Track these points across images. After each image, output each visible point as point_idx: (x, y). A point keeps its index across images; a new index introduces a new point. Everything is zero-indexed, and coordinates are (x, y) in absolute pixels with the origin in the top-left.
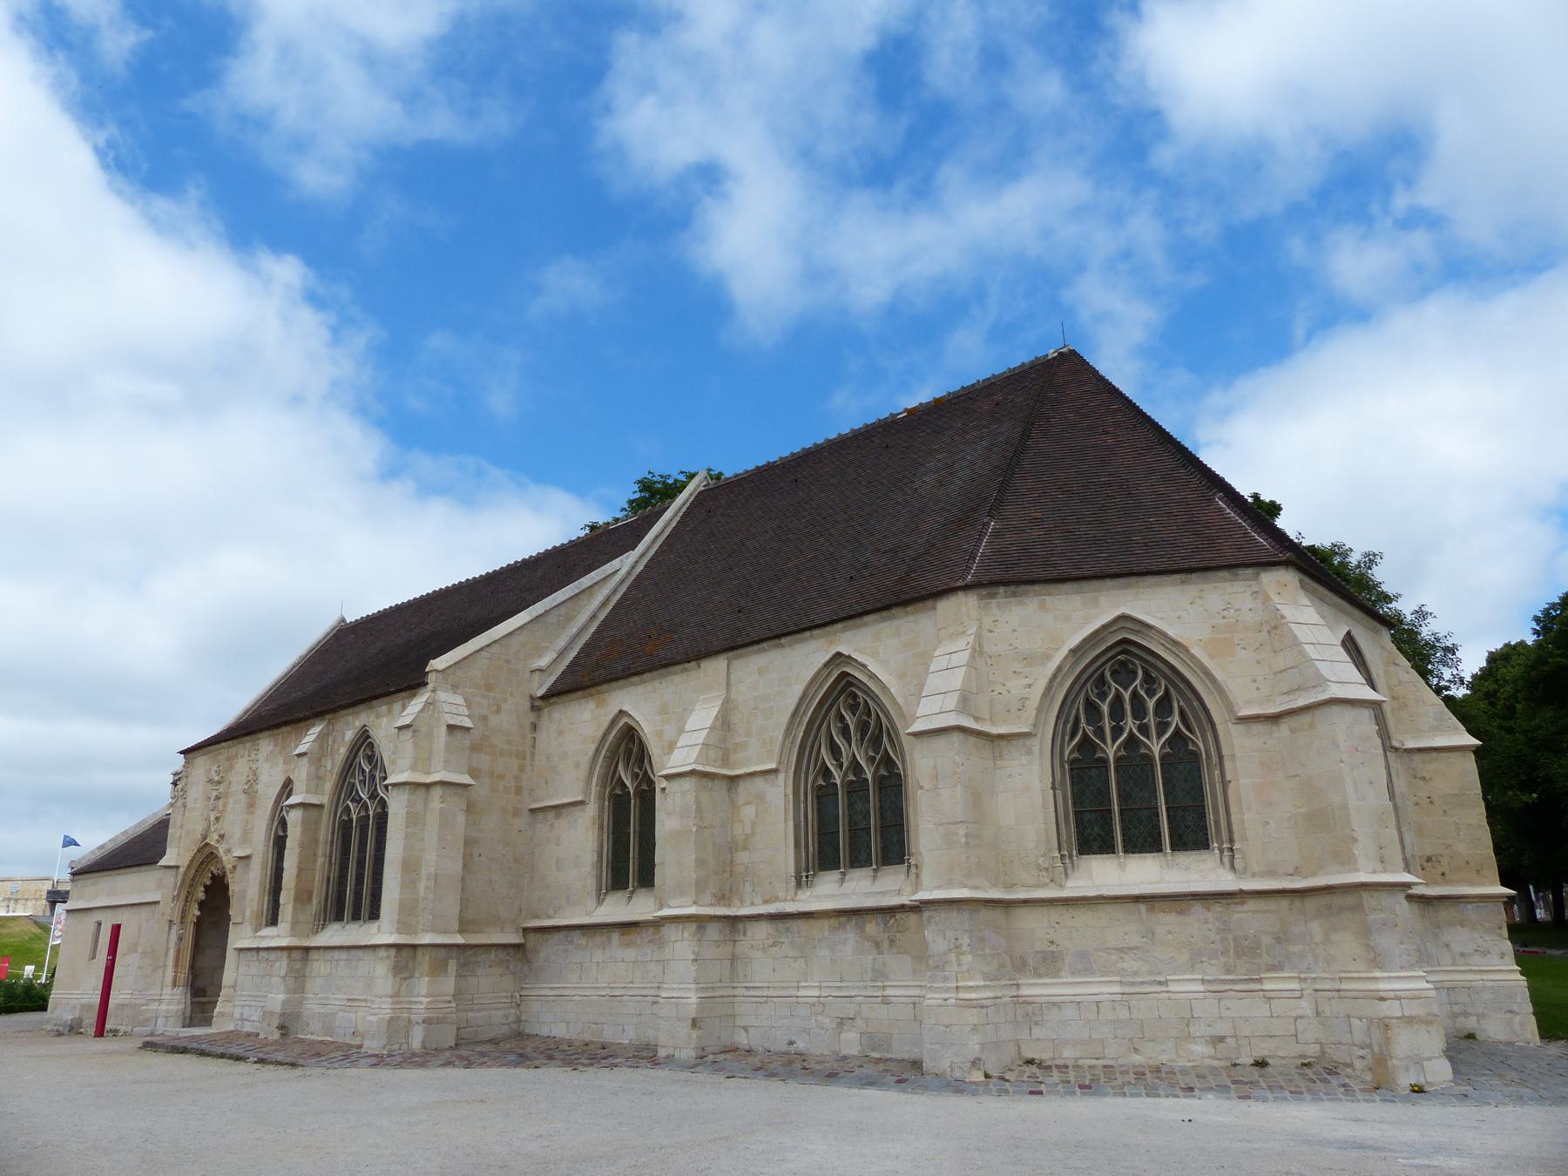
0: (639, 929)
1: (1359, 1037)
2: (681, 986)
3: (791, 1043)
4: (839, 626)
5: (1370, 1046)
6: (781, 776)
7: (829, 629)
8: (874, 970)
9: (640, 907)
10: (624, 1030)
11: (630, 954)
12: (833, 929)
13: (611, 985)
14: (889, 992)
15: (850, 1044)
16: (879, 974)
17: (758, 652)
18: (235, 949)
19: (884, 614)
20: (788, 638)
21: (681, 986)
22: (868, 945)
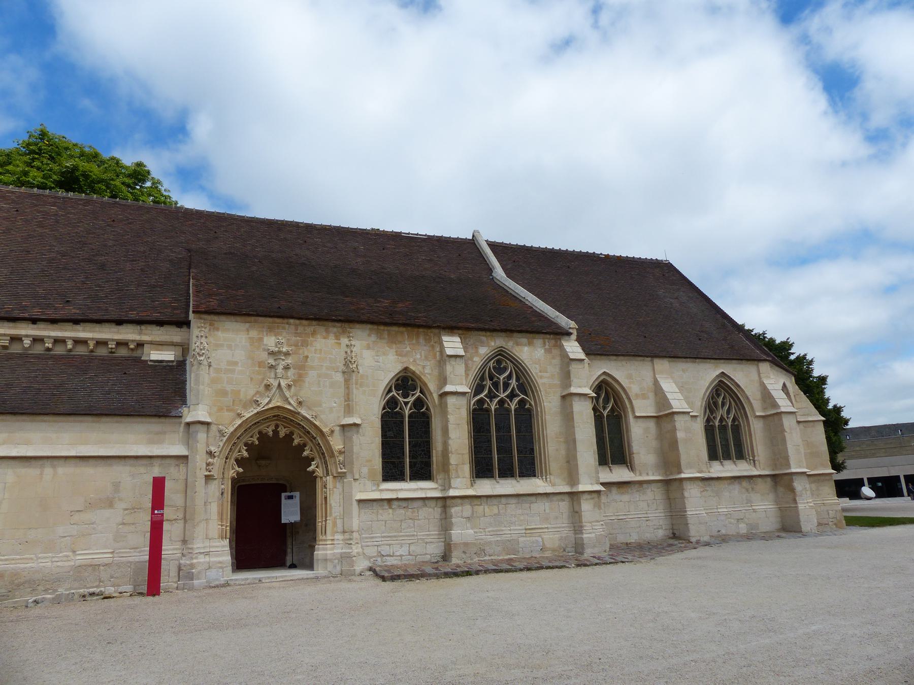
0: (629, 485)
1: (831, 516)
2: (698, 509)
3: (719, 531)
4: (722, 361)
5: (836, 518)
6: (698, 419)
7: (718, 361)
8: (747, 500)
9: (620, 474)
10: (630, 536)
11: (626, 498)
12: (729, 484)
13: (615, 514)
14: (754, 508)
15: (743, 528)
16: (749, 501)
17: (683, 362)
18: (356, 500)
19: (740, 361)
20: (700, 360)
21: (698, 509)
22: (744, 490)
